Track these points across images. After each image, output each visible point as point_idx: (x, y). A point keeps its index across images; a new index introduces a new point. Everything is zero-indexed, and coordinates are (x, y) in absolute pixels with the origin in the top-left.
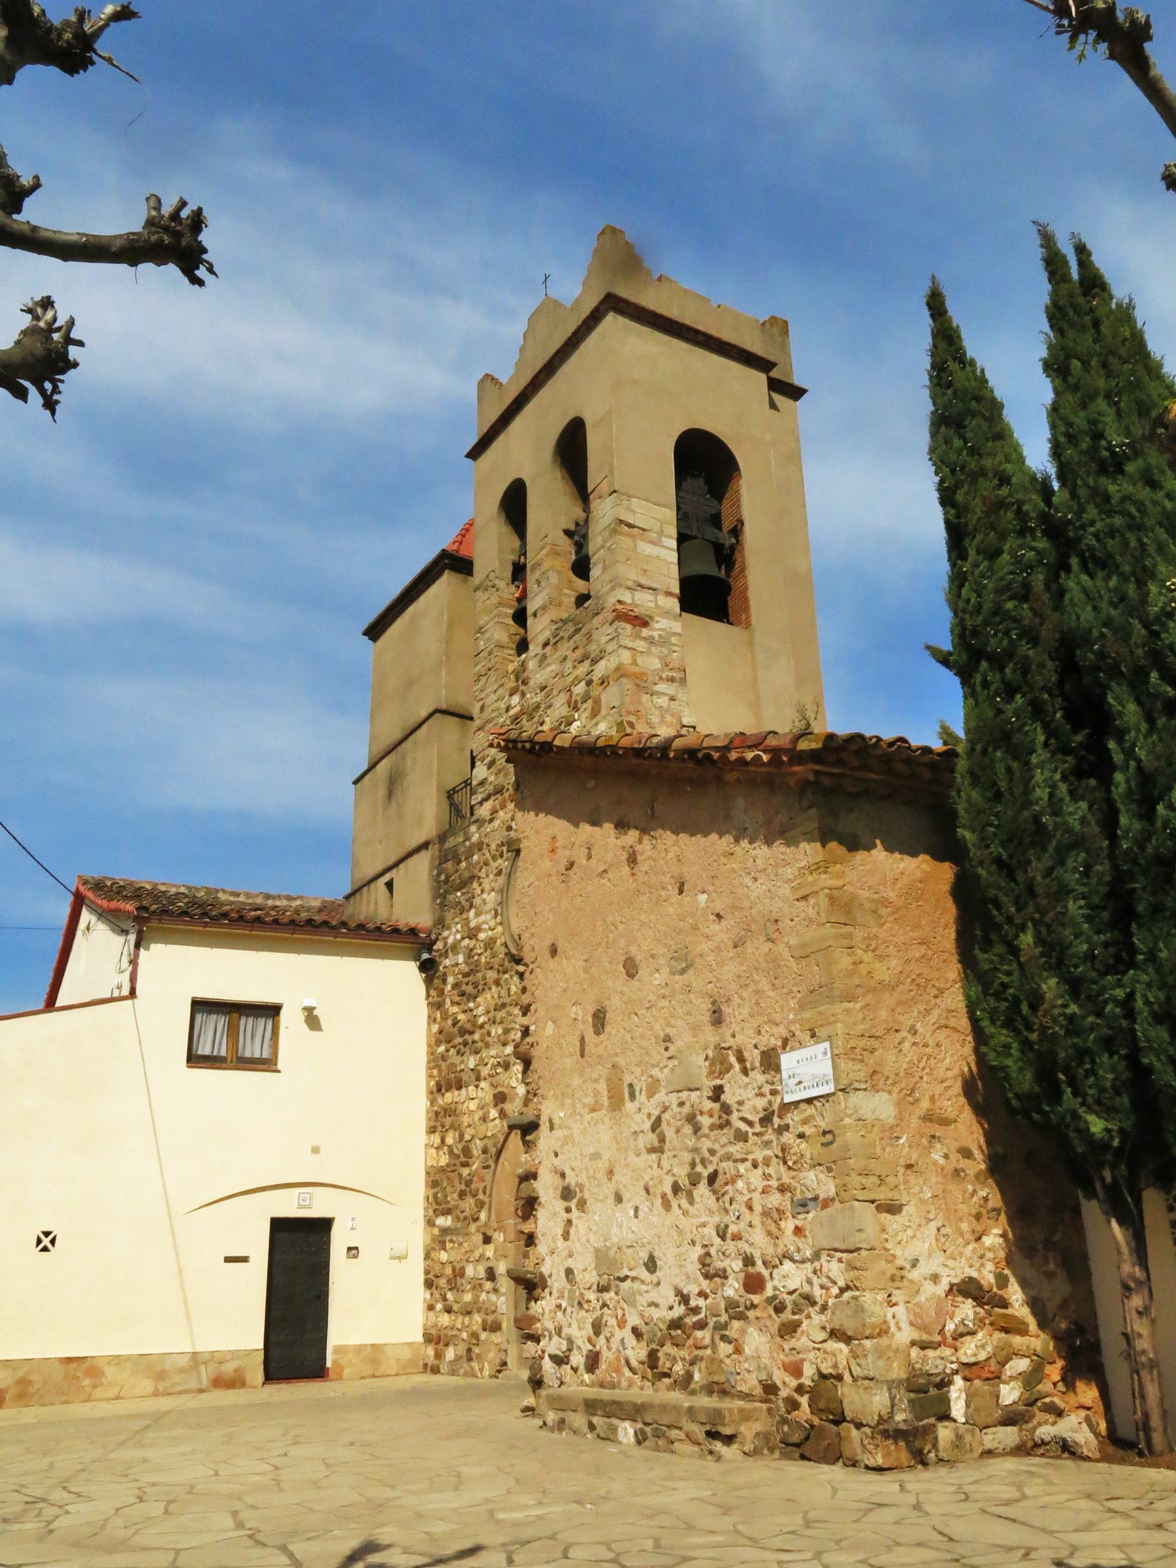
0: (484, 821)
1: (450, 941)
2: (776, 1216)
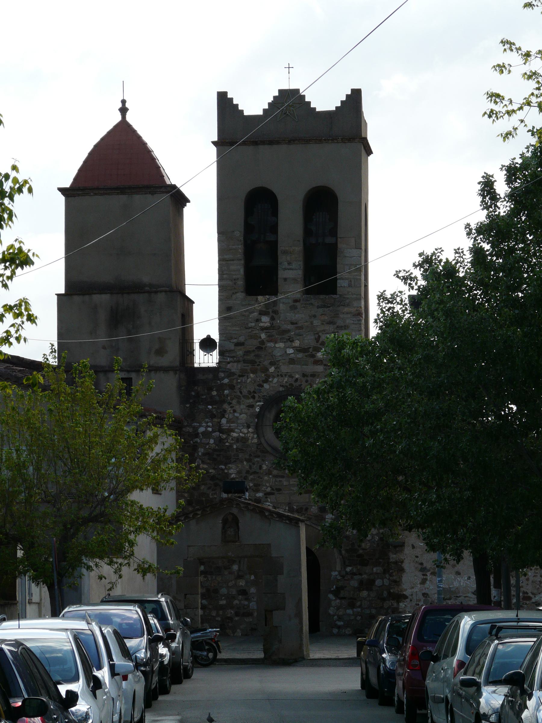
0: (233, 374)
1: (202, 429)
2: (538, 583)
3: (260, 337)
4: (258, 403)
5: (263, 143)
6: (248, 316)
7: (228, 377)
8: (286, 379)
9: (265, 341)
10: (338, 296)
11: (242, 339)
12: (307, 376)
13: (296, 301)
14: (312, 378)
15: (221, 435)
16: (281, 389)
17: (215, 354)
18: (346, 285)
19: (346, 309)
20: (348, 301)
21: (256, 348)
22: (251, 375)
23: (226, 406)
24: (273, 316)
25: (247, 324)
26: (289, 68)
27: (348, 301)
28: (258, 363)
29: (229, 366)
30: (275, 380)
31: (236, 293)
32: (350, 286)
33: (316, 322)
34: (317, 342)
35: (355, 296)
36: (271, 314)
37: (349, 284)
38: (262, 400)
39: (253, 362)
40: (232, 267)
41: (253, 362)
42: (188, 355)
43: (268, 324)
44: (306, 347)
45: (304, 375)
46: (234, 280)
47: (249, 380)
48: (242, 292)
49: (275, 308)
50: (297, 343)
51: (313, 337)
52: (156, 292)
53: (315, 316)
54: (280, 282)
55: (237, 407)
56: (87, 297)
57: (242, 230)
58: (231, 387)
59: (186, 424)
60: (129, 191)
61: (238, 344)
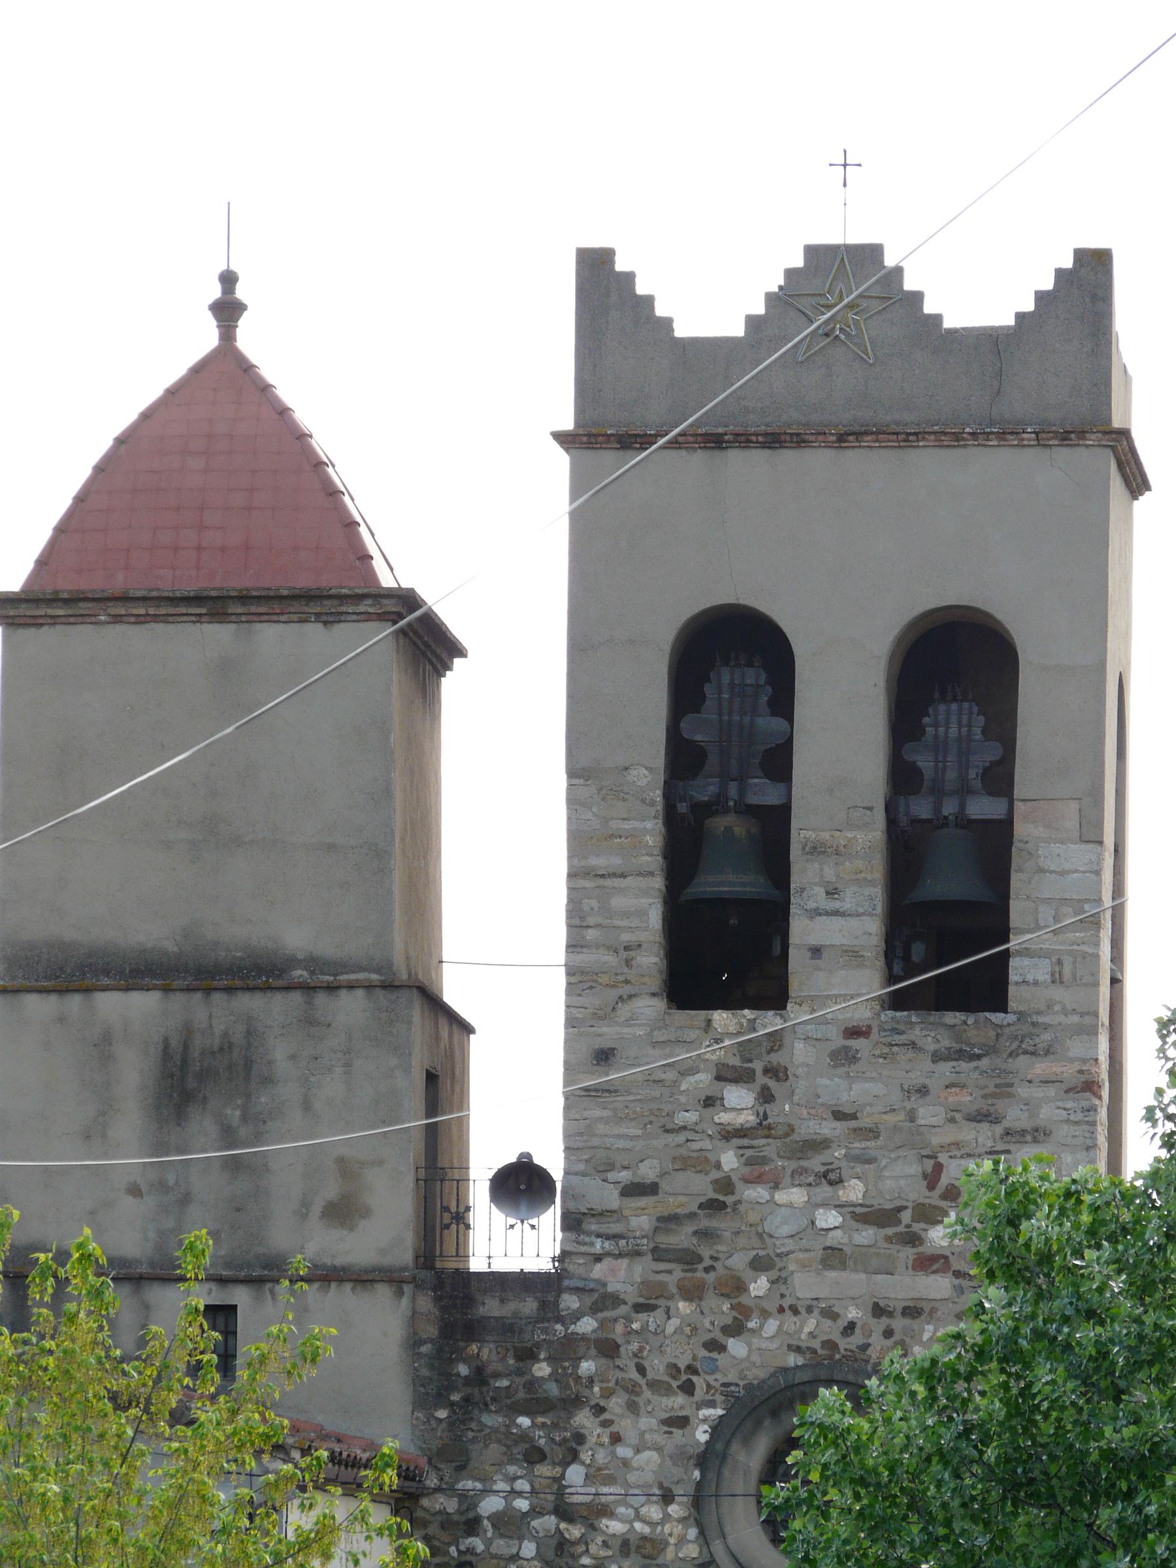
0: (615, 1300)
1: (491, 1505)
3: (718, 1166)
4: (705, 1412)
5: (743, 440)
6: (675, 1084)
7: (595, 1309)
8: (811, 1324)
9: (735, 1179)
10: (1011, 1018)
11: (648, 1171)
12: (890, 1314)
13: (854, 1032)
14: (907, 1322)
15: (563, 1526)
16: (793, 1360)
17: (550, 1220)
18: (1041, 979)
19: (1041, 1068)
20: (1047, 1036)
21: (701, 1206)
22: (681, 1305)
23: (583, 1419)
24: (768, 1089)
25: (670, 1115)
26: (845, 165)
27: (1047, 1036)
28: (707, 1262)
29: (599, 1271)
30: (772, 1326)
31: (630, 997)
32: (1057, 979)
33: (929, 1114)
34: (931, 1187)
35: (1076, 1019)
36: (761, 1079)
37: (1053, 975)
38: (719, 1398)
39: (689, 1259)
40: (617, 902)
41: (689, 1259)
42: (447, 1227)
43: (747, 1118)
44: (888, 1206)
45: (879, 1311)
46: (626, 948)
47: (672, 1325)
48: (654, 995)
49: (776, 1059)
50: (854, 1191)
51: (914, 1169)
52: (332, 988)
53: (923, 1091)
54: (797, 960)
55: (625, 1425)
56: (75, 1002)
57: (659, 760)
58: (608, 1349)
59: (432, 1482)
60: (240, 611)
61: (634, 1190)
